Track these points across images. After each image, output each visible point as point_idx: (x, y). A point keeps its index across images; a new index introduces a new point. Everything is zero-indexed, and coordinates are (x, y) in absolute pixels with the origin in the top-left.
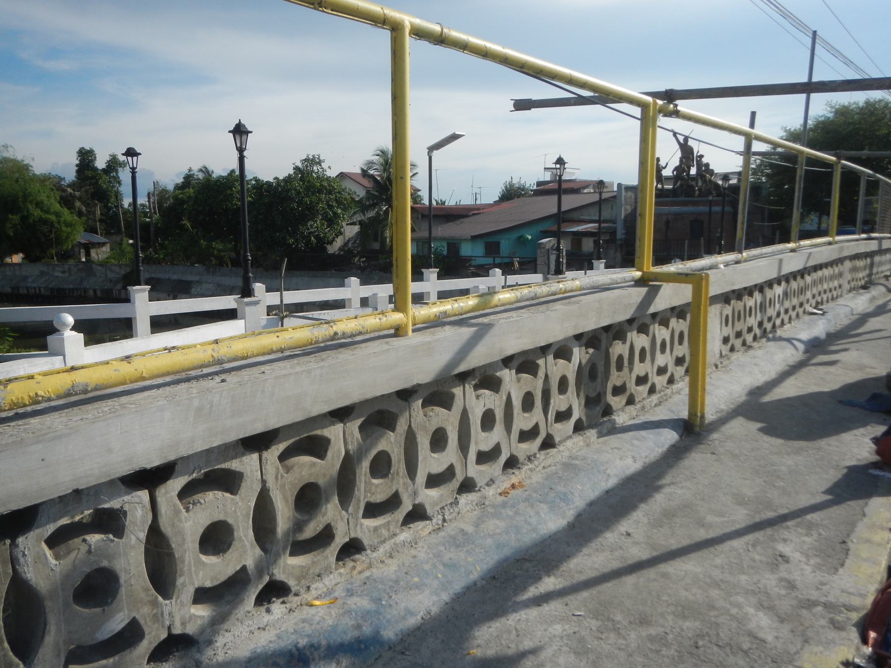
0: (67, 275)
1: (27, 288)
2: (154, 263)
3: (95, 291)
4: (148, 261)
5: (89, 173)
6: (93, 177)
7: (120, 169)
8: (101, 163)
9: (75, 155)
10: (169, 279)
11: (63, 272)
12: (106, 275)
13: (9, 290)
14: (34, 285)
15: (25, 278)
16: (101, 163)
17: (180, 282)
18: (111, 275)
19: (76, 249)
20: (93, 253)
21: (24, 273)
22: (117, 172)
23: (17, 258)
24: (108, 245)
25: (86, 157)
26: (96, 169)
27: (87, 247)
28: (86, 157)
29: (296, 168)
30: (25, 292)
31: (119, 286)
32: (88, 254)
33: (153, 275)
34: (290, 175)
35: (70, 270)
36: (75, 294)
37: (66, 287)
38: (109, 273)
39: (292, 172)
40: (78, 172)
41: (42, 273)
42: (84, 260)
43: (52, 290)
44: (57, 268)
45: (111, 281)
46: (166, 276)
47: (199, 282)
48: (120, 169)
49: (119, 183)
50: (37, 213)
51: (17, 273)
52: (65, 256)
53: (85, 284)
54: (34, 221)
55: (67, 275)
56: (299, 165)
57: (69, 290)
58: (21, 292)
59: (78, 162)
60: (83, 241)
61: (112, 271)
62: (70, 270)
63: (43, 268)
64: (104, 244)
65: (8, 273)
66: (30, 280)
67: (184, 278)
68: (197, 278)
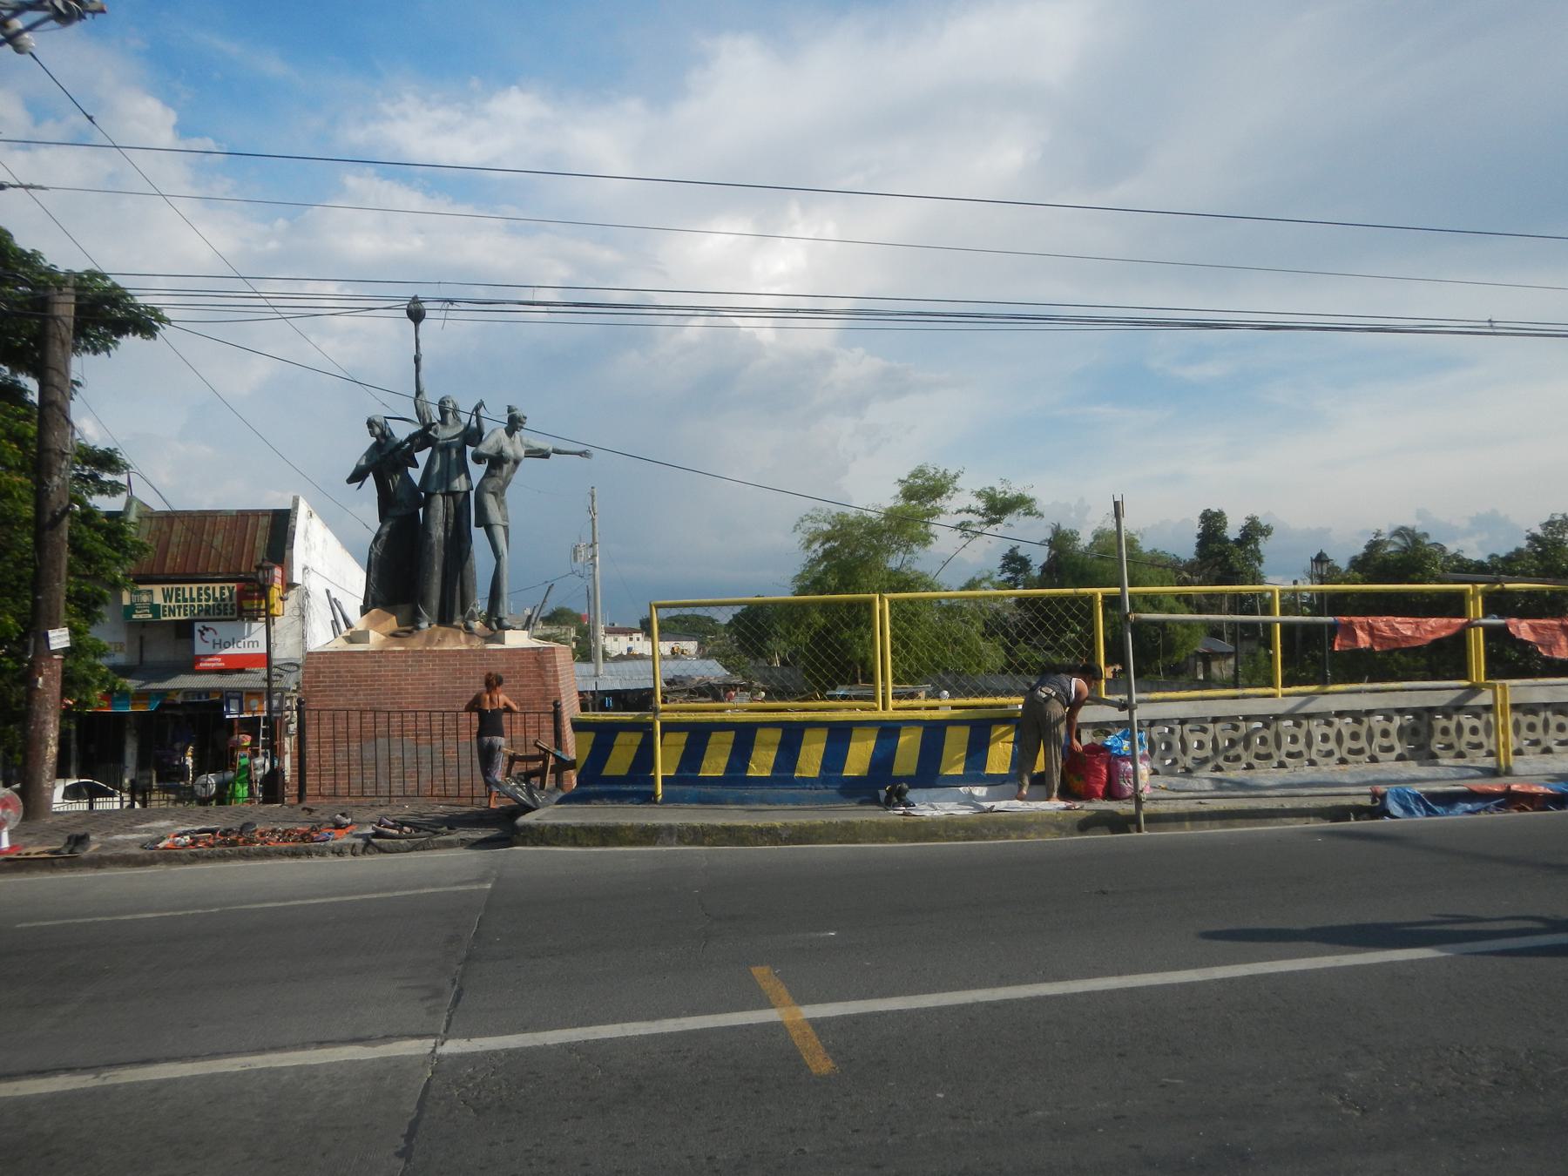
5: (1215, 547)
6: (1221, 553)
7: (1261, 539)
8: (1233, 531)
9: (1197, 521)
16: (1233, 531)
19: (1192, 661)
22: (1256, 544)
25: (1212, 523)
26: (1226, 540)
27: (1207, 658)
28: (1212, 523)
29: (1534, 538)
32: (1207, 669)
34: (1519, 551)
39: (1524, 544)
40: (1199, 545)
42: (1201, 677)
48: (1261, 539)
49: (1260, 560)
56: (1539, 532)
59: (1199, 531)
60: (1201, 649)
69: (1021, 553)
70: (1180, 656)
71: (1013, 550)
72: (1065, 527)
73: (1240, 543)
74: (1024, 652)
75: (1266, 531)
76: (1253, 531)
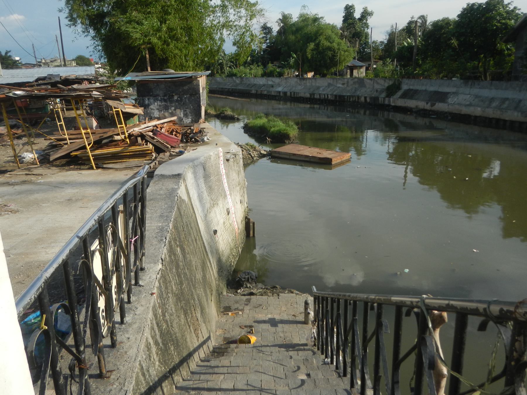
0: (345, 86)
1: (320, 95)
2: (414, 77)
3: (365, 98)
4: (410, 76)
5: (350, 21)
6: (353, 24)
8: (357, 15)
10: (426, 90)
11: (343, 84)
12: (374, 87)
13: (308, 95)
14: (324, 93)
15: (318, 88)
16: (357, 15)
17: (436, 93)
18: (377, 87)
19: (345, 70)
20: (355, 72)
21: (317, 85)
22: (367, 20)
23: (310, 75)
24: (364, 68)
25: (349, 10)
27: (352, 68)
28: (349, 10)
30: (318, 97)
31: (383, 95)
33: (411, 87)
35: (348, 82)
36: (351, 99)
37: (345, 94)
38: (375, 85)
41: (329, 85)
43: (336, 96)
44: (339, 81)
45: (377, 91)
46: (423, 88)
47: (456, 94)
50: (327, 44)
51: (313, 84)
52: (342, 74)
53: (358, 93)
54: (323, 49)
55: (345, 86)
57: (347, 96)
58: (315, 97)
59: (344, 15)
60: (349, 65)
61: (378, 83)
62: (348, 82)
63: (331, 81)
64: (361, 67)
65: (308, 84)
66: (321, 89)
67: (440, 90)
68: (454, 90)
69: (269, 25)
70: (341, 67)
71: (265, 24)
72: (286, 13)
73: (360, 19)
74: (271, 67)
75: (371, 14)
76: (366, 14)
